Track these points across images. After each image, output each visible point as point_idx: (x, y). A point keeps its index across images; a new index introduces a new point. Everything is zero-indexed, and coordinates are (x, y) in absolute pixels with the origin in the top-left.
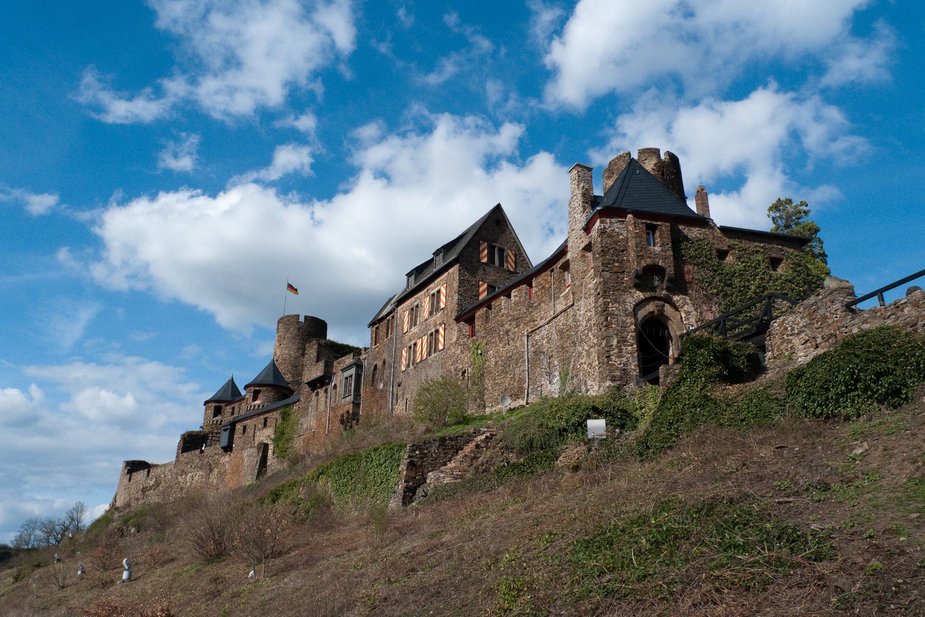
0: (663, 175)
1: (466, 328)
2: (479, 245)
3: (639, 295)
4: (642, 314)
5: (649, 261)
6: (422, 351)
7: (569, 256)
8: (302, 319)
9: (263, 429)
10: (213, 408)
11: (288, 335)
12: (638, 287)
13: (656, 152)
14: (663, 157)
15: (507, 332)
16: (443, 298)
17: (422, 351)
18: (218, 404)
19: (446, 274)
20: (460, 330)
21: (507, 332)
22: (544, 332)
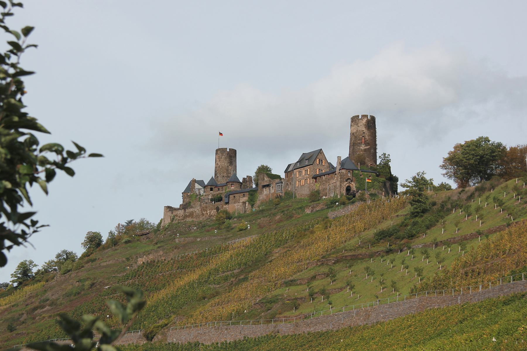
0: (368, 124)
1: (314, 180)
2: (317, 160)
3: (346, 183)
4: (347, 185)
5: (348, 178)
6: (303, 183)
7: (336, 173)
8: (228, 150)
9: (243, 197)
10: (209, 188)
11: (223, 157)
12: (346, 181)
13: (366, 116)
14: (369, 118)
15: (324, 183)
16: (308, 172)
17: (303, 183)
18: (211, 187)
19: (309, 166)
20: (313, 180)
21: (324, 183)
22: (331, 185)
